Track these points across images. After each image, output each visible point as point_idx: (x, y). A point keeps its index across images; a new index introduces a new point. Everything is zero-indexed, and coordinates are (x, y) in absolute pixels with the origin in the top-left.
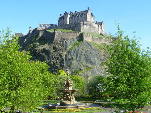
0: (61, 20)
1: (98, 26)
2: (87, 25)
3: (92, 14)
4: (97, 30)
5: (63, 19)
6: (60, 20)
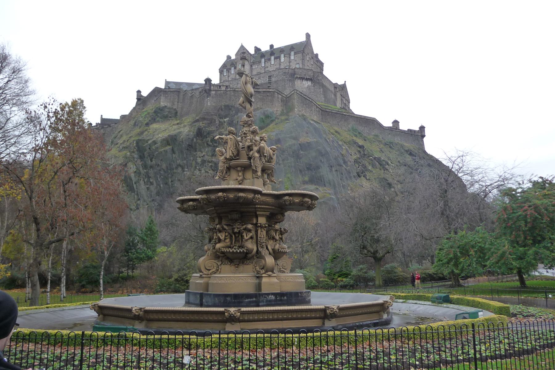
0: (228, 70)
1: (335, 88)
2: (302, 79)
3: (317, 55)
4: (333, 96)
5: (233, 68)
6: (225, 70)
